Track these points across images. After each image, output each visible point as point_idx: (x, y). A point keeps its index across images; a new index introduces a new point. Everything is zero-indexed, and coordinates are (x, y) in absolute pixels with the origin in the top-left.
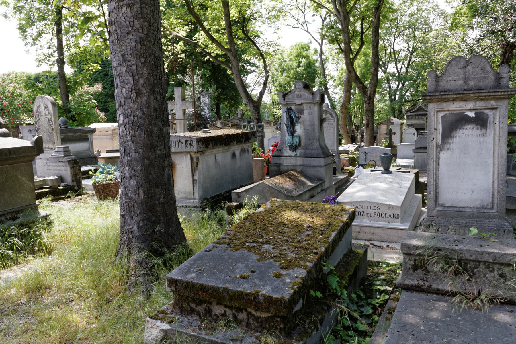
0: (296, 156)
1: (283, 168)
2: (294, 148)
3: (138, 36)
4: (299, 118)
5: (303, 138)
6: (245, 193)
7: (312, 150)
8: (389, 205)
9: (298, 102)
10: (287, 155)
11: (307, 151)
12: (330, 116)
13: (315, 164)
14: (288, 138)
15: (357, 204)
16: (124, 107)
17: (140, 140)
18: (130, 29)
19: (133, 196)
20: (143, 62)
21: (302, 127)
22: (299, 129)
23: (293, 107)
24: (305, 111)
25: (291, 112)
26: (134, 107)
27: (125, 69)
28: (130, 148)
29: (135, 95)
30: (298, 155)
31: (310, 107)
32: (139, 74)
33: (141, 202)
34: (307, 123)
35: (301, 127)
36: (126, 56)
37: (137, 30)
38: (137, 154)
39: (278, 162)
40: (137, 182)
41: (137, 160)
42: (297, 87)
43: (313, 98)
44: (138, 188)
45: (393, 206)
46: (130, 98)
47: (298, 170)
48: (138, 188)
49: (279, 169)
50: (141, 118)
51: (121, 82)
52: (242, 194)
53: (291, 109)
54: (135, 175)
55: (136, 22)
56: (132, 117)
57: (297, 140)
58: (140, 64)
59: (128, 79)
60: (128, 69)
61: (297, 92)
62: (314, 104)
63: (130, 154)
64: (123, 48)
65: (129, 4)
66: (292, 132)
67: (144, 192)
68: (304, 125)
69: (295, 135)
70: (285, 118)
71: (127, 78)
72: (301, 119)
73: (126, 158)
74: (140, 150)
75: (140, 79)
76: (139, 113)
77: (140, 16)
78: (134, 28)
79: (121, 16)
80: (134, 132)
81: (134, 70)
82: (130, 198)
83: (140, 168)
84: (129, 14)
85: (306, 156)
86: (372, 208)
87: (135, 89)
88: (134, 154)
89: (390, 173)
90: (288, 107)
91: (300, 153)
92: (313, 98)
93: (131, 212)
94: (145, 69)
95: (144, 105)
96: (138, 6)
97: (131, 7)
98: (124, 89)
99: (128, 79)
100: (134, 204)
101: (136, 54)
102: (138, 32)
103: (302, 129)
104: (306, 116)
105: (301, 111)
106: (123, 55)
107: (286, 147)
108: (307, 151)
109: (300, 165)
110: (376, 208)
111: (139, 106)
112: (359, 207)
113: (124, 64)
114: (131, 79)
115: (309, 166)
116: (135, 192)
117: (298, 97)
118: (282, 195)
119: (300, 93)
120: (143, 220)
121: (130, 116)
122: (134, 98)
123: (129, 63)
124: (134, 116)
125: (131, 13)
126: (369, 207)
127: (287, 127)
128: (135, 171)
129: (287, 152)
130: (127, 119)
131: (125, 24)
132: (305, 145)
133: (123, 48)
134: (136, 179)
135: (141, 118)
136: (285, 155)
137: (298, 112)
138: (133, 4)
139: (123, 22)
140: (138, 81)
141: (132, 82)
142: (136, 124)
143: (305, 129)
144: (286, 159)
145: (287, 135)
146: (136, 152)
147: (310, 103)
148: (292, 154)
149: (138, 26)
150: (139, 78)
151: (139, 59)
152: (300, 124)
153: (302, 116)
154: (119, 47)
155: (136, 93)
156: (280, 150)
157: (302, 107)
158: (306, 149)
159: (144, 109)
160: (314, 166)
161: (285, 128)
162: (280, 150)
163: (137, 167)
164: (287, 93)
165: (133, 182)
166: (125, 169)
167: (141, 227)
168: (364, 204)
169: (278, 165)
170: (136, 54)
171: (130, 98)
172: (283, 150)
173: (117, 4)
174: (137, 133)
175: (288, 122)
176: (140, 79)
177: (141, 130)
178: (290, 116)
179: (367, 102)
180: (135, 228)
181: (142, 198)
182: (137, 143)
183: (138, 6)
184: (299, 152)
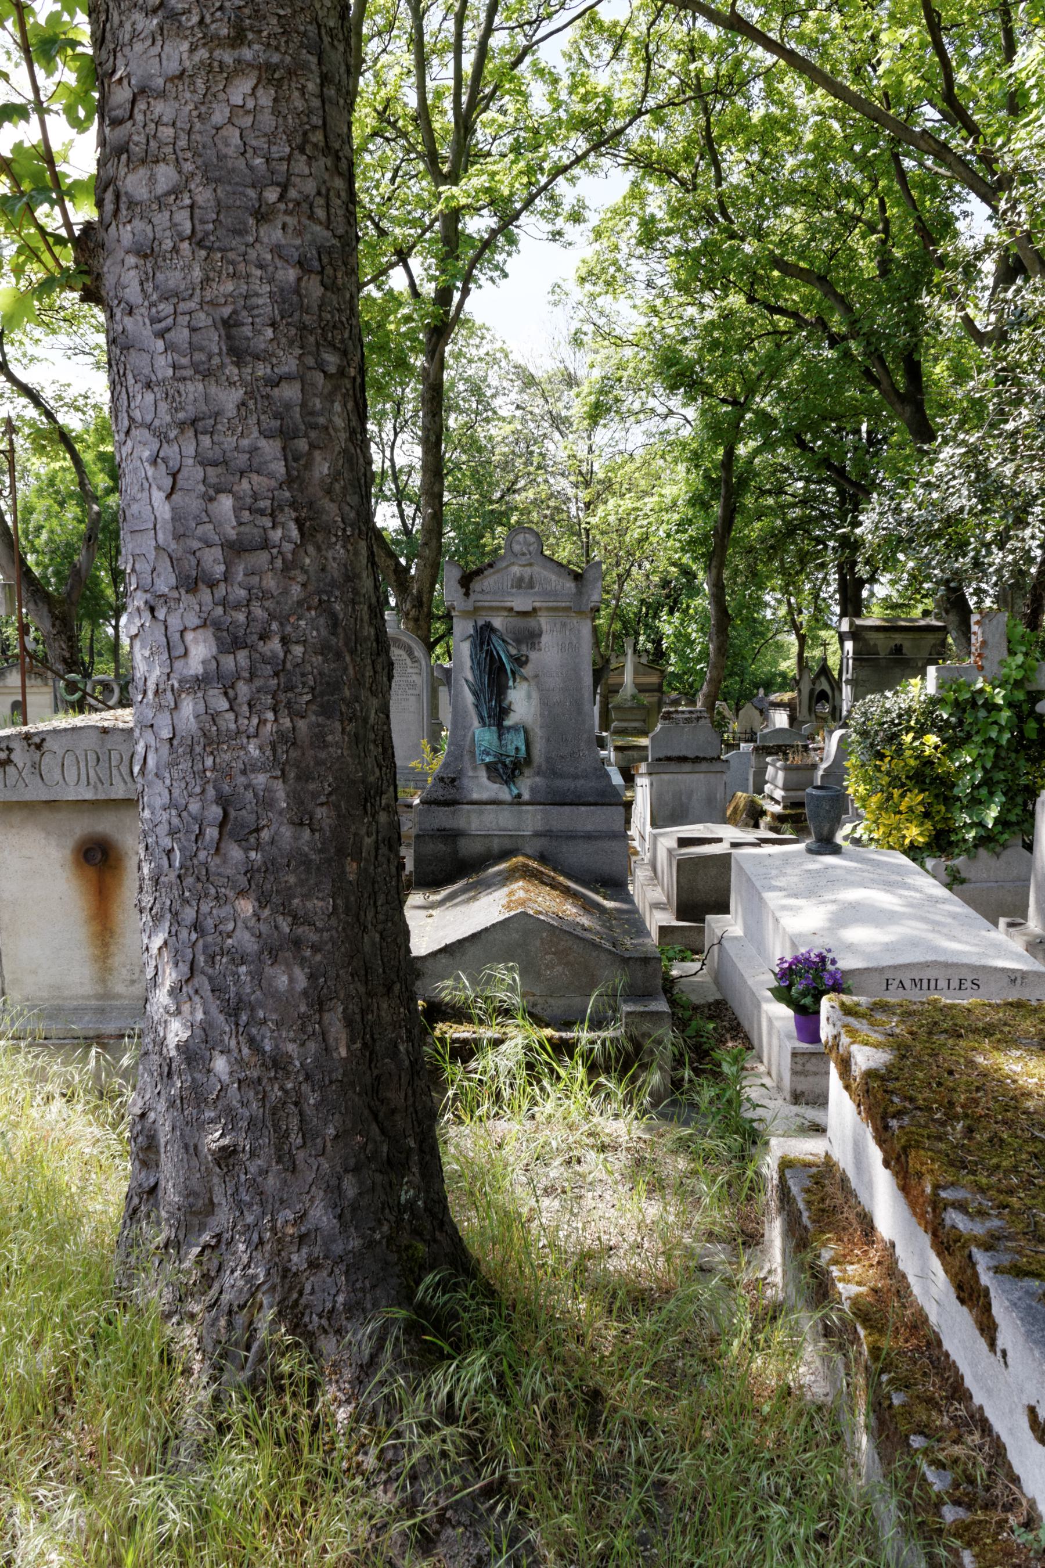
1: (468, 848)
2: (506, 770)
3: (308, 237)
4: (521, 661)
5: (538, 735)
6: (444, 960)
7: (576, 777)
8: (1013, 971)
9: (521, 603)
10: (485, 796)
11: (559, 783)
12: (405, 656)
13: (589, 827)
14: (484, 737)
15: (900, 975)
16: (221, 590)
17: (319, 763)
18: (272, 195)
19: (291, 1048)
20: (332, 369)
21: (535, 695)
22: (522, 703)
23: (497, 623)
24: (545, 639)
25: (494, 639)
26: (286, 592)
27: (237, 394)
28: (266, 802)
29: (295, 533)
30: (526, 796)
31: (564, 625)
32: (314, 426)
33: (338, 1075)
34: (554, 682)
35: (529, 697)
36: (247, 331)
37: (305, 206)
38: (307, 834)
40: (312, 977)
41: (306, 862)
42: (516, 548)
43: (580, 593)
44: (320, 1005)
45: (1024, 974)
46: (265, 545)
47: (529, 851)
48: (320, 1005)
49: (456, 852)
50: (324, 649)
51: (203, 462)
52: (429, 964)
53: (488, 627)
54: (297, 943)
55: (301, 165)
56: (275, 645)
57: (518, 741)
58: (319, 378)
59: (253, 450)
60: (257, 395)
61: (516, 570)
62: (580, 613)
63: (265, 835)
64: (229, 287)
65: (269, 68)
66: (496, 714)
67: (349, 1022)
68: (540, 689)
69: (507, 723)
70: (468, 663)
71: (245, 442)
73: (235, 852)
74: (321, 813)
75: (317, 455)
76: (309, 626)
77: (318, 137)
78: (293, 193)
79: (220, 115)
80: (286, 722)
81: (288, 406)
82: (278, 1063)
83: (319, 905)
84: (267, 120)
85: (558, 799)
86: (955, 984)
87: (294, 505)
88: (287, 832)
89: (836, 850)
90: (481, 623)
91: (533, 790)
92: (580, 593)
93: (287, 1135)
94: (337, 407)
95: (333, 584)
96: (311, 86)
97: (278, 84)
98: (226, 503)
99: (253, 450)
100: (298, 1091)
101: (303, 328)
102: (311, 217)
103: (535, 701)
104: (549, 654)
105: (532, 638)
106: (229, 324)
107: (475, 769)
108: (559, 783)
109: (537, 835)
110: (968, 984)
111: (311, 588)
112: (907, 984)
113: (232, 370)
114: (271, 448)
115: (571, 836)
116: (303, 1029)
117: (519, 587)
118: (603, 957)
119: (528, 569)
120: (356, 1170)
121: (264, 637)
122: (288, 547)
123: (262, 370)
124: (285, 641)
125: (276, 112)
126: (943, 984)
127: (475, 694)
128: (296, 919)
129: (482, 786)
130: (242, 655)
131: (241, 163)
132: (548, 760)
133: (229, 287)
134: (303, 962)
135: (324, 649)
136: (475, 796)
137: (518, 641)
138: (291, 73)
139: (230, 151)
140: (309, 465)
141: (279, 468)
142: (296, 680)
144: (481, 812)
145: (476, 723)
146: (302, 820)
147: (568, 609)
148: (504, 793)
149: (310, 187)
150: (312, 446)
151: (317, 355)
153: (533, 655)
154: (206, 280)
155: (299, 523)
156: (453, 780)
157: (532, 623)
158: (552, 772)
159: (337, 607)
160: (589, 837)
161: (469, 698)
162: (453, 780)
163: (305, 897)
164: (479, 572)
165: (287, 979)
166: (225, 911)
167: (355, 1208)
168: (926, 974)
169: (451, 836)
170: (303, 328)
171: (265, 545)
172: (466, 782)
173: (203, 53)
174: (302, 724)
175: (479, 678)
176: (317, 455)
177: (326, 711)
179: (413, 613)
180: (321, 1216)
181: (344, 1053)
182: (304, 776)
183: (311, 86)
184: (525, 786)
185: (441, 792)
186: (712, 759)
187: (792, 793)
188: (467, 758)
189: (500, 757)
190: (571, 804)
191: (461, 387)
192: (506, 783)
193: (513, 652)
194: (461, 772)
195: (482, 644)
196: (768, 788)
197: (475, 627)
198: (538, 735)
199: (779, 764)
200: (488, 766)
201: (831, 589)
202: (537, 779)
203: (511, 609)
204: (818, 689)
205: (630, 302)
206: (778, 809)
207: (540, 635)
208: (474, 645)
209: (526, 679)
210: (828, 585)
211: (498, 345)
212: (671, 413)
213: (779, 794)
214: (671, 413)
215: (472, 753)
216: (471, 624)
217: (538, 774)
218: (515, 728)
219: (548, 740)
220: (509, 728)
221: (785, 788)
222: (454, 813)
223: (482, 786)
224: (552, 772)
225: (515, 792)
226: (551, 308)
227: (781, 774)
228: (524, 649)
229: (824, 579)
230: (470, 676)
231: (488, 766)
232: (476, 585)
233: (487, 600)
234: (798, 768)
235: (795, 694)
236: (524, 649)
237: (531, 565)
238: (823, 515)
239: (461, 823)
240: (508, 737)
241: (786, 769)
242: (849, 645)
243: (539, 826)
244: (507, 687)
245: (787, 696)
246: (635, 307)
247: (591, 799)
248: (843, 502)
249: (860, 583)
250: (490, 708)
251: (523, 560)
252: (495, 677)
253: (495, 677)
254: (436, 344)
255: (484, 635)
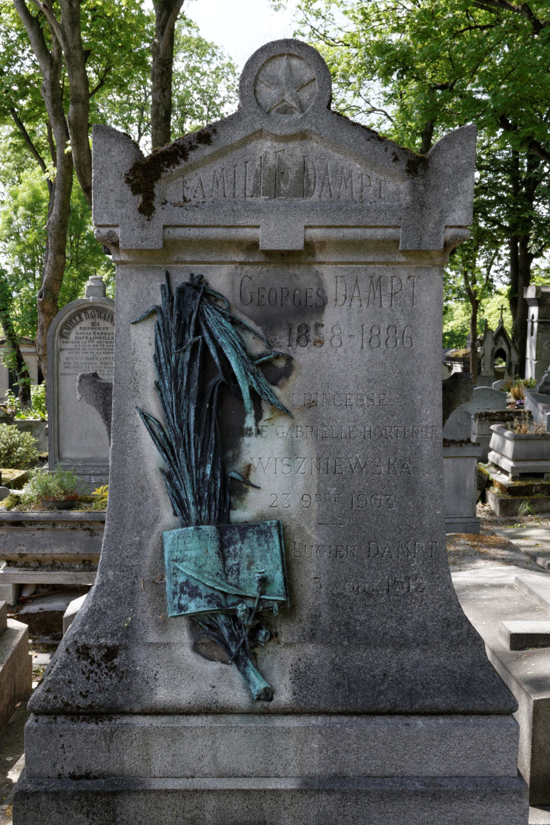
0: (264, 705)
2: (236, 630)
4: (272, 369)
5: (312, 538)
7: (401, 643)
9: (277, 231)
11: (360, 657)
13: (435, 768)
14: (187, 551)
21: (306, 448)
22: (276, 467)
23: (219, 279)
24: (331, 317)
25: (212, 317)
30: (284, 696)
31: (378, 283)
35: (292, 453)
39: (98, 761)
42: (269, 94)
43: (420, 205)
53: (198, 287)
61: (265, 147)
62: (417, 254)
66: (213, 490)
68: (320, 438)
69: (240, 515)
70: (149, 374)
72: (295, 381)
90: (180, 279)
91: (301, 677)
92: (420, 205)
103: (306, 464)
104: (340, 354)
105: (301, 314)
107: (163, 625)
108: (360, 657)
109: (310, 787)
117: (274, 192)
119: (296, 149)
127: (165, 446)
129: (177, 671)
132: (335, 600)
136: (163, 695)
137: (269, 324)
143: (328, 467)
144: (177, 734)
145: (167, 515)
148: (230, 686)
152: (283, 426)
153: (303, 356)
156: (111, 653)
157: (302, 278)
158: (343, 630)
161: (152, 457)
162: (111, 653)
172: (142, 658)
175: (174, 409)
178: (201, 352)
184: (281, 668)
185: (81, 684)
186: (462, 442)
187: (521, 464)
188: (144, 599)
189: (223, 605)
190: (391, 713)
191: (196, 96)
192: (237, 660)
193: (257, 348)
194: (129, 633)
195: (182, 329)
196: (492, 456)
197: (167, 289)
198: (312, 538)
199: (507, 433)
200: (195, 621)
201: (502, 262)
202: (310, 649)
203: (252, 246)
204: (499, 347)
205: (342, 9)
206: (505, 479)
207: (320, 308)
208: (162, 331)
209: (286, 412)
210: (500, 258)
211: (226, 61)
212: (373, 110)
213: (507, 464)
214: (373, 110)
215: (158, 585)
216: (158, 281)
217: (312, 637)
218: (257, 528)
219: (336, 554)
220: (245, 528)
221: (515, 459)
222: (110, 737)
223: (177, 671)
224: (343, 630)
225: (259, 685)
226: (272, 11)
227: (509, 446)
228: (282, 343)
229: (496, 254)
230: (154, 408)
231: (195, 621)
232: (168, 188)
233: (195, 224)
234: (528, 438)
235: (469, 349)
236: (282, 343)
237: (303, 136)
238: (500, 199)
239: (129, 760)
240: (243, 548)
241: (516, 439)
242: (534, 311)
243: (315, 765)
244: (243, 432)
245: (461, 352)
246: (345, 13)
247: (440, 702)
248: (517, 188)
249: (531, 257)
250: (199, 484)
251: (285, 125)
252: (210, 410)
253: (210, 410)
254: (166, 20)
255: (186, 313)
